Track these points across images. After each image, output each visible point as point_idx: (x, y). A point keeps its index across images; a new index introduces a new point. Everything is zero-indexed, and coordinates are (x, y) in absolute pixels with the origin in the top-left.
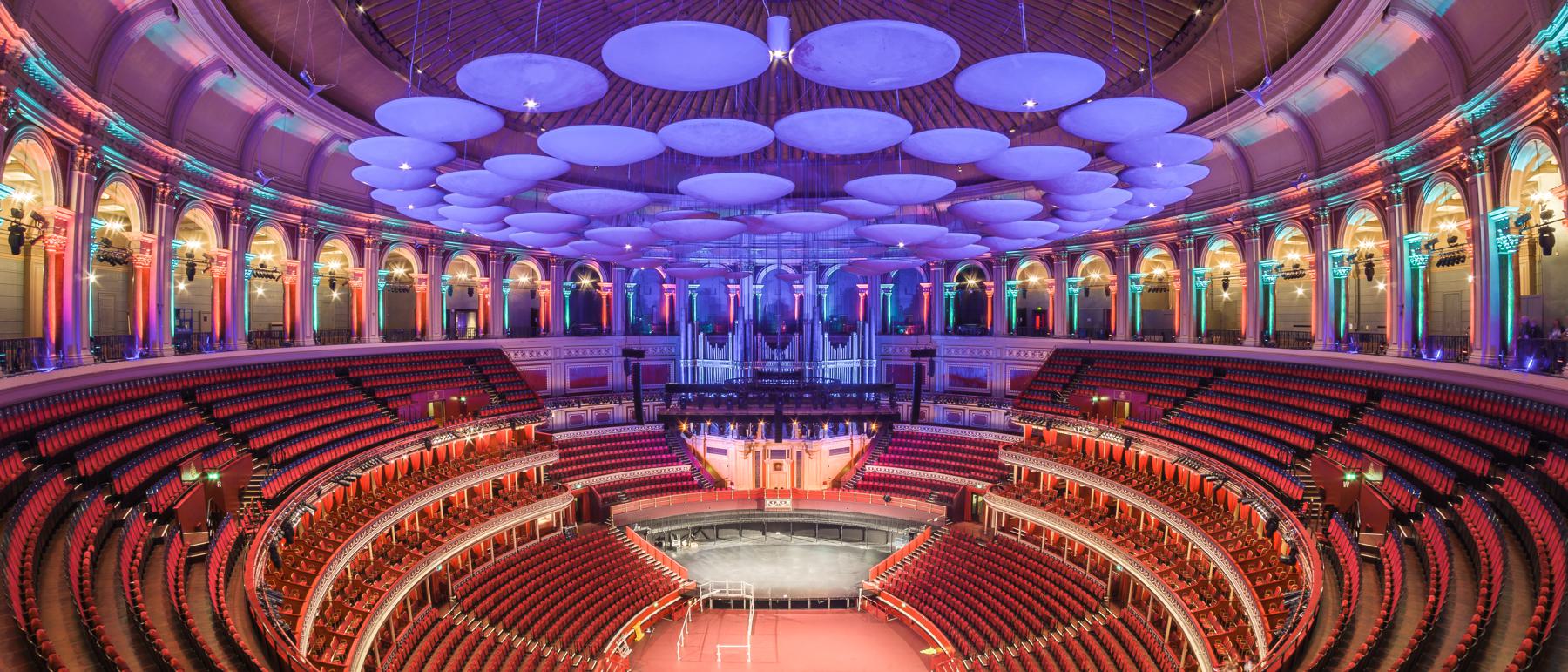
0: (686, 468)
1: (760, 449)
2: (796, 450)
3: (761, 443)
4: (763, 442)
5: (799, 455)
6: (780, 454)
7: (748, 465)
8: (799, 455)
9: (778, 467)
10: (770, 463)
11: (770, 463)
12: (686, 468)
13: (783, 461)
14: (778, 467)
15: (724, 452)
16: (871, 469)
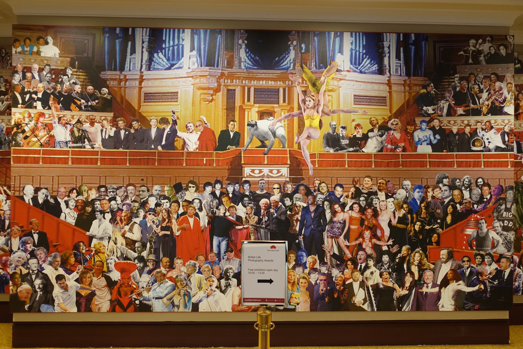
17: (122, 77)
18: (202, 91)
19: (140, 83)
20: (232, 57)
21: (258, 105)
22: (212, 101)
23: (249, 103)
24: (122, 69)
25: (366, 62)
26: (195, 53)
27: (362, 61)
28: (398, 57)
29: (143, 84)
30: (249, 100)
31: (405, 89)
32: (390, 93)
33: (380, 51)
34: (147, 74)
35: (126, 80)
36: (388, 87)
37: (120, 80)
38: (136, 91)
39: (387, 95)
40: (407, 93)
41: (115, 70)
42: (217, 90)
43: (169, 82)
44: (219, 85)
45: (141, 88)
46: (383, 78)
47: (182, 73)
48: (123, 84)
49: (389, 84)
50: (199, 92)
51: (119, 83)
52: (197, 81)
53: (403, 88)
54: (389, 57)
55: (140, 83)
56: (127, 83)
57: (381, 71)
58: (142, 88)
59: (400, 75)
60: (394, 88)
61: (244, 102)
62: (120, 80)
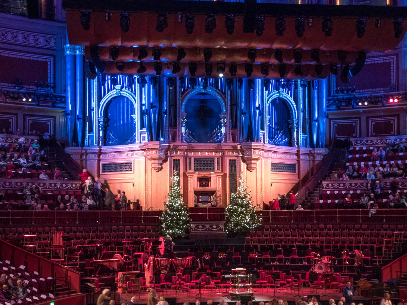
8: (233, 165)
15: (127, 167)
17: (84, 151)
18: (153, 161)
19: (99, 156)
20: (175, 133)
21: (197, 172)
23: (190, 171)
25: (278, 136)
26: (144, 130)
27: (275, 136)
28: (304, 132)
29: (101, 157)
30: (190, 169)
31: (310, 158)
32: (298, 161)
33: (290, 127)
34: (104, 148)
35: (87, 154)
36: (296, 157)
37: (82, 154)
38: (96, 163)
39: (295, 162)
40: (311, 162)
41: (77, 146)
42: (165, 161)
43: (124, 155)
44: (167, 157)
45: (99, 160)
46: (294, 150)
47: (136, 146)
48: (84, 157)
49: (298, 154)
50: (150, 162)
51: (81, 157)
52: (148, 153)
53: (308, 157)
54: (297, 132)
55: (99, 156)
56: (88, 156)
57: (290, 143)
58: (100, 160)
59: (306, 147)
60: (302, 157)
61: (186, 171)
62: (82, 154)
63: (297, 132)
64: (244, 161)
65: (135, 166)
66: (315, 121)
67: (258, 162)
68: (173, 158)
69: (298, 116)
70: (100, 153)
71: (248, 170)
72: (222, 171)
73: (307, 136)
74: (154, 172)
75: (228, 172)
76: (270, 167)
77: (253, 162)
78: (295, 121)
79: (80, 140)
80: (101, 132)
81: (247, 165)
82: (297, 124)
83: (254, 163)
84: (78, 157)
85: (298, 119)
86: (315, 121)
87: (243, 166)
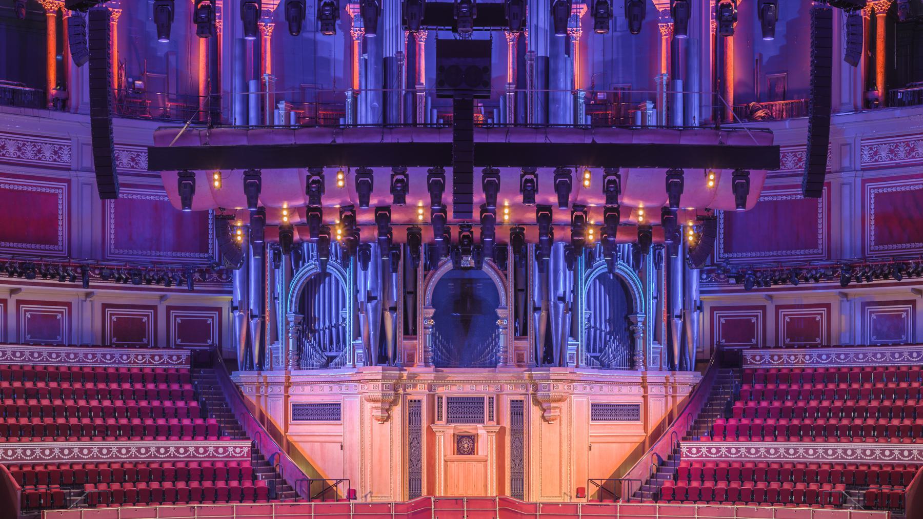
0: (237, 449)
1: (419, 392)
2: (511, 393)
3: (423, 380)
4: (426, 374)
5: (518, 409)
6: (467, 409)
7: (389, 437)
8: (518, 409)
9: (465, 445)
10: (445, 435)
11: (445, 435)
12: (237, 449)
13: (481, 431)
14: (465, 445)
15: (331, 412)
16: (700, 450)
17: (261, 380)
19: (287, 388)
21: (453, 425)
22: (389, 417)
24: (261, 366)
28: (657, 338)
29: (291, 390)
35: (268, 384)
38: (281, 401)
41: (251, 368)
42: (394, 403)
48: (263, 390)
50: (368, 405)
51: (258, 389)
54: (644, 339)
55: (287, 388)
56: (269, 389)
58: (288, 396)
61: (433, 422)
63: (644, 339)
64: (537, 402)
65: (345, 413)
66: (677, 316)
67: (564, 405)
68: (409, 398)
69: (647, 310)
70: (288, 385)
71: (545, 420)
72: (498, 423)
73: (664, 346)
74: (376, 424)
75: (507, 423)
76: (587, 412)
77: (553, 405)
78: (640, 317)
79: (256, 360)
80: (292, 342)
81: (544, 410)
82: (644, 324)
83: (555, 408)
84: (253, 389)
85: (645, 313)
86: (677, 316)
87: (535, 412)
